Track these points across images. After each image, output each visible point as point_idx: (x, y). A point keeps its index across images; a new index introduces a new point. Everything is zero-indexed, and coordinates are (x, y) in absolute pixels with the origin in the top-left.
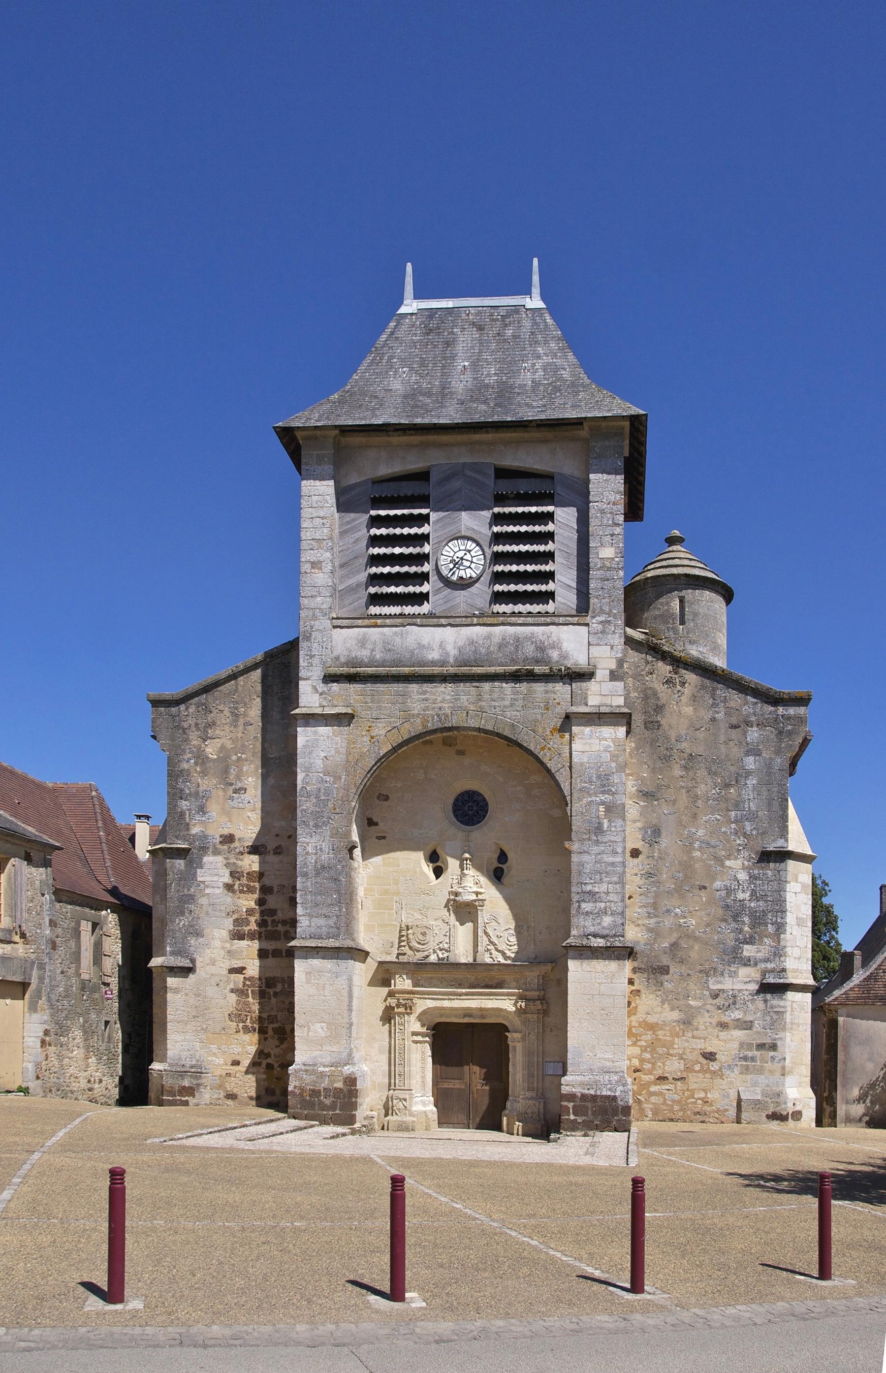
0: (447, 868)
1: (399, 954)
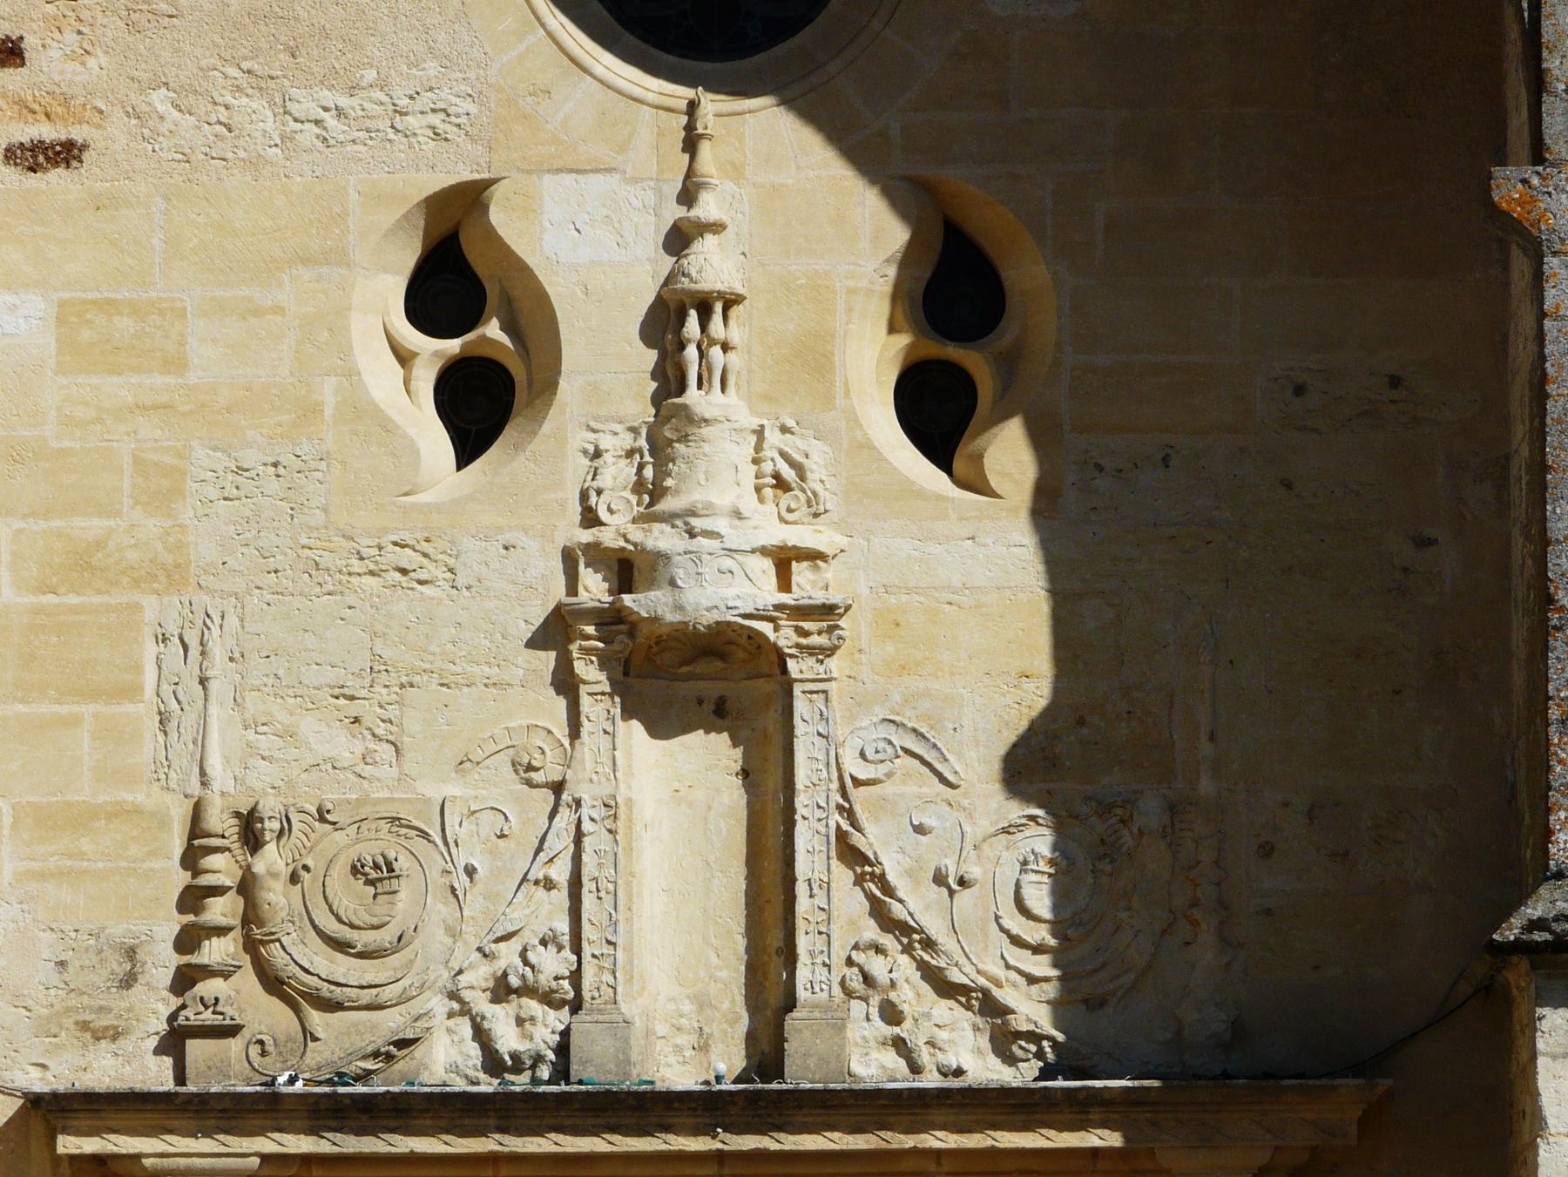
0: (551, 386)
1: (174, 1041)
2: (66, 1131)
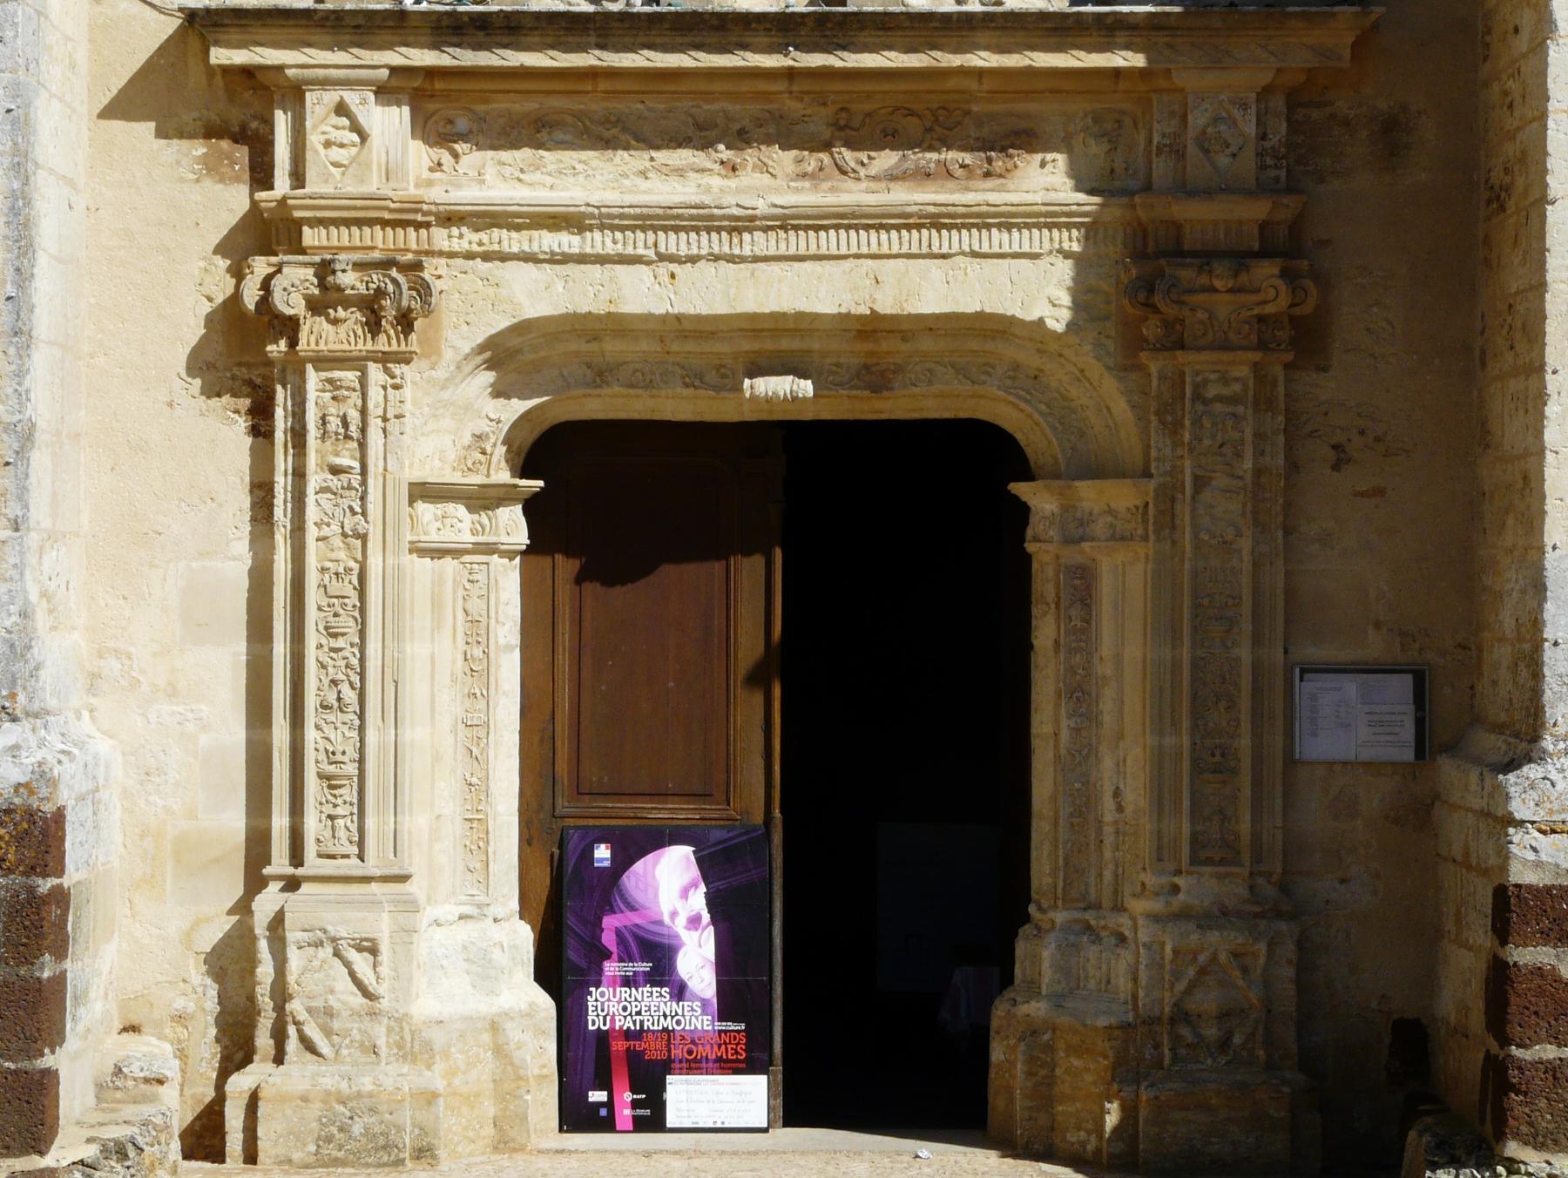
2: (217, 43)
